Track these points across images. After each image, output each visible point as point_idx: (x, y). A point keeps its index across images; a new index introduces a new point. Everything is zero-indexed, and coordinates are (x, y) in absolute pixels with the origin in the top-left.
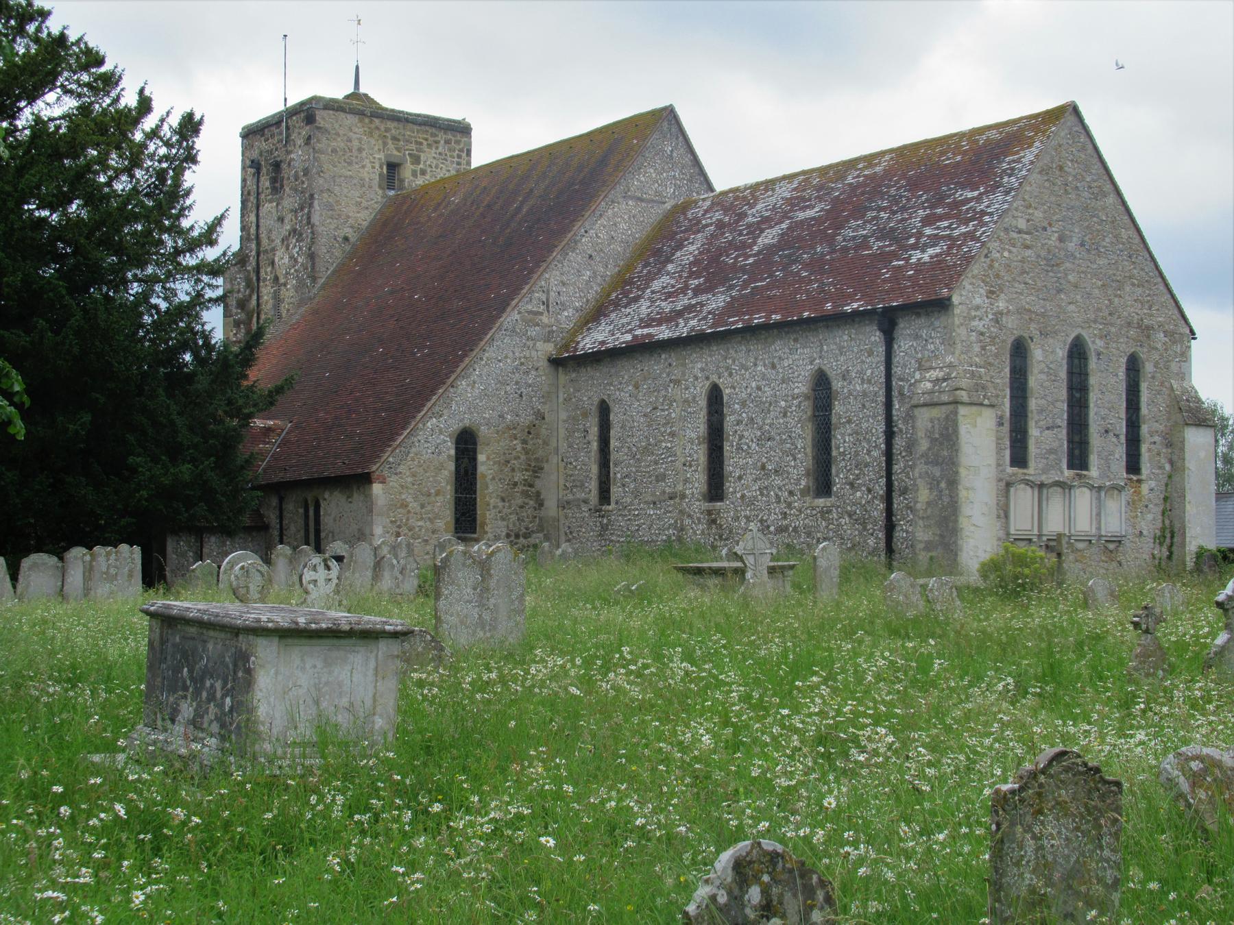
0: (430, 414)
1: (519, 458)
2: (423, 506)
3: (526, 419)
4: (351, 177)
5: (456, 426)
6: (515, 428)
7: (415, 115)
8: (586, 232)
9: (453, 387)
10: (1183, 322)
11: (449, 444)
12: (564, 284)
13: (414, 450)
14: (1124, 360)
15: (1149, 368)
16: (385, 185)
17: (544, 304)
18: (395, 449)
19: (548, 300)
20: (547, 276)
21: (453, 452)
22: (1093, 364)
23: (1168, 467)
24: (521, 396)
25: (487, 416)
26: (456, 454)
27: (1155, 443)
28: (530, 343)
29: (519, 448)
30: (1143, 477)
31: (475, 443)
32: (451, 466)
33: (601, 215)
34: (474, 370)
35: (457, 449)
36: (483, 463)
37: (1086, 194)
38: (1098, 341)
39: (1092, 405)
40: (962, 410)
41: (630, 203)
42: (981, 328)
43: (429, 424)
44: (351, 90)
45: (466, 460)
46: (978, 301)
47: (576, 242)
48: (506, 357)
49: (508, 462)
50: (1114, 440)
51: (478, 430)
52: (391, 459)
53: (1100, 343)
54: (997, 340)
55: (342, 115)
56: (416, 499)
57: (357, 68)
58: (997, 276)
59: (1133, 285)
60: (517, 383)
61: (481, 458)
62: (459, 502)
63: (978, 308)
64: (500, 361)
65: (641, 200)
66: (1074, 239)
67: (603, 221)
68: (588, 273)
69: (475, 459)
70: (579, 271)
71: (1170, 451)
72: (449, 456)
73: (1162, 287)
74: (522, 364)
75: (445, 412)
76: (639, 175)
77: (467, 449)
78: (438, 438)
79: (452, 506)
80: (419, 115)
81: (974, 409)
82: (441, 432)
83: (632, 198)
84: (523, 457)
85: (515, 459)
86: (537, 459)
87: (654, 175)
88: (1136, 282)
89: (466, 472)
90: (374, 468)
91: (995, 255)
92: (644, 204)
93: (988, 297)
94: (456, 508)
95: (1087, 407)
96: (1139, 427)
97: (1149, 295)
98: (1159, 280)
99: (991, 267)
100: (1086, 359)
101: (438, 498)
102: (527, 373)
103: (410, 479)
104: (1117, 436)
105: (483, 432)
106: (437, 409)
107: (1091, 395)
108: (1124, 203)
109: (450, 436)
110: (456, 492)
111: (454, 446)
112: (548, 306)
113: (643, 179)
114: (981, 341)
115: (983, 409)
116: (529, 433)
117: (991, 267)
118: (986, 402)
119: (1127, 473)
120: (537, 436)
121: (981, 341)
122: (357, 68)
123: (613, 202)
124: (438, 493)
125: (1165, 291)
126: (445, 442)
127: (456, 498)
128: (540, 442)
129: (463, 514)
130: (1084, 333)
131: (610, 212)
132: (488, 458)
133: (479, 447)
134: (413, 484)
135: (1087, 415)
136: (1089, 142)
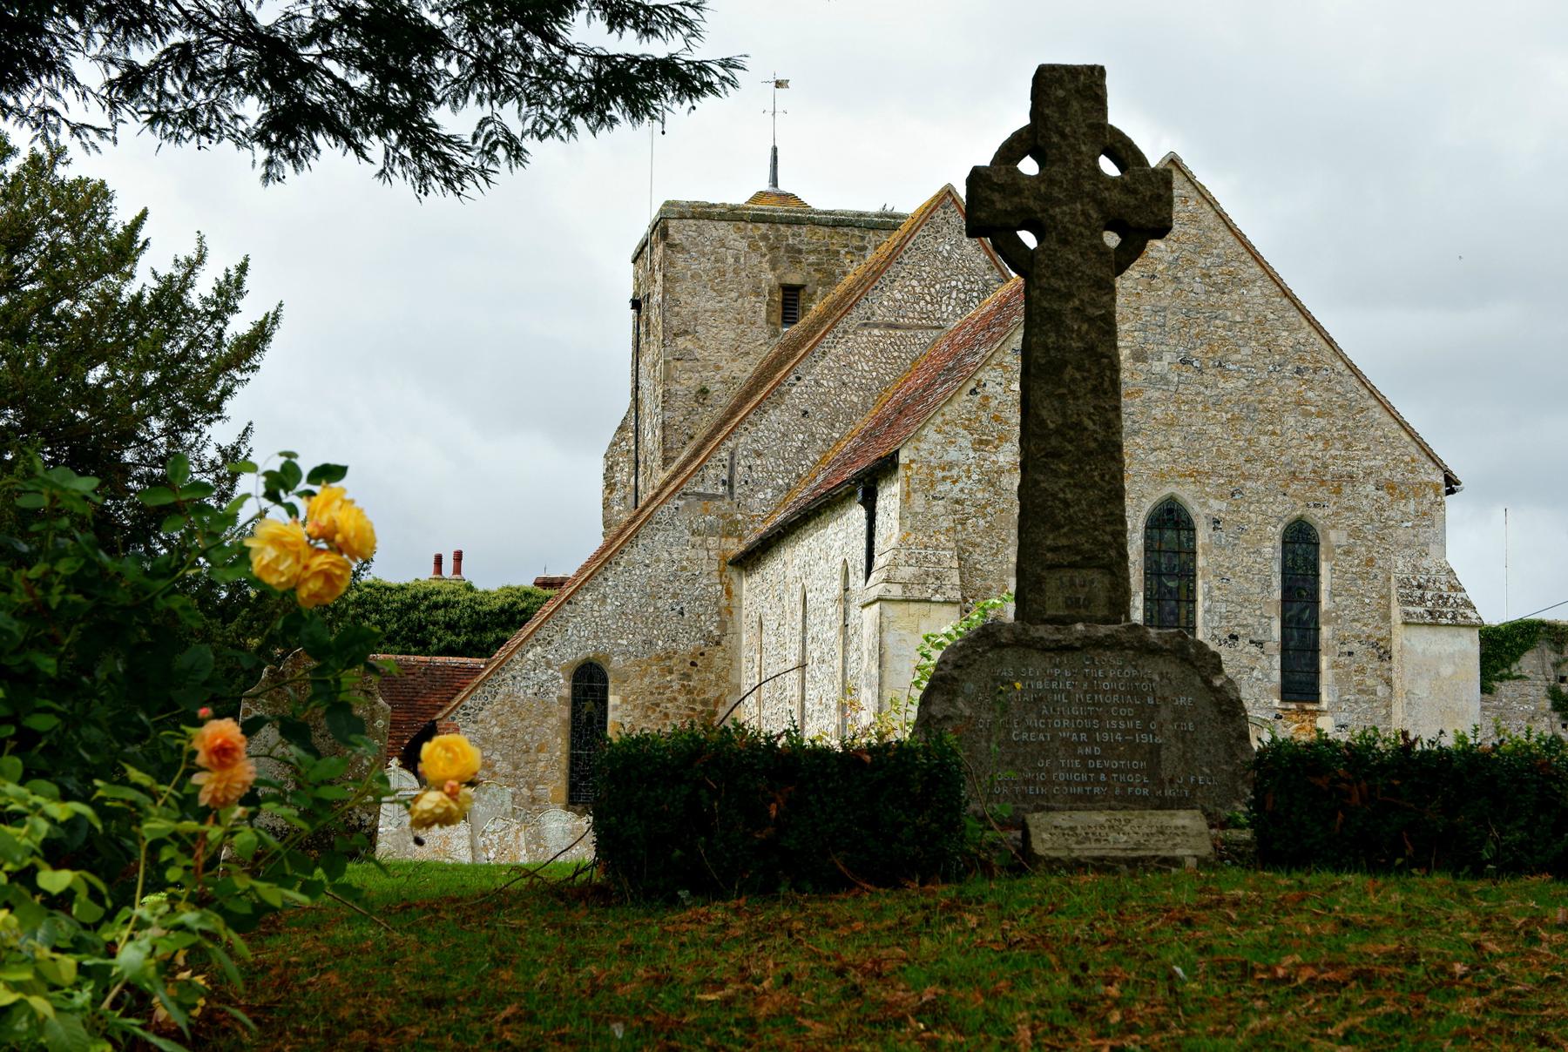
0: (532, 640)
1: (675, 699)
2: (516, 767)
3: (687, 645)
4: (722, 310)
5: (573, 654)
6: (670, 658)
7: (825, 213)
8: (798, 379)
9: (570, 603)
10: (1431, 464)
11: (562, 681)
12: (759, 455)
13: (504, 689)
14: (1275, 532)
15: (1333, 538)
16: (776, 318)
17: (724, 483)
18: (475, 688)
19: (731, 477)
20: (730, 444)
21: (567, 692)
22: (1203, 535)
23: (1381, 690)
24: (682, 614)
25: (625, 642)
26: (574, 694)
27: (1350, 654)
28: (698, 540)
29: (676, 686)
30: (1324, 705)
31: (606, 680)
32: (566, 714)
33: (824, 353)
34: (606, 579)
35: (574, 688)
36: (616, 708)
37: (1197, 287)
38: (1212, 502)
39: (1200, 598)
40: (892, 610)
41: (876, 332)
42: (956, 493)
43: (530, 655)
44: (765, 186)
45: (589, 705)
46: (953, 454)
47: (781, 395)
48: (658, 560)
49: (658, 705)
50: (1254, 649)
51: (608, 659)
52: (468, 703)
53: (1217, 506)
54: (989, 509)
55: (710, 224)
56: (504, 756)
57: (775, 150)
58: (997, 419)
59: (1307, 414)
60: (675, 595)
61: (613, 700)
62: (574, 761)
63: (951, 465)
64: (647, 566)
65: (897, 327)
66: (1167, 357)
67: (828, 361)
68: (801, 436)
69: (605, 702)
70: (784, 435)
71: (1386, 665)
72: (560, 698)
73: (1378, 413)
74: (684, 568)
75: (557, 637)
76: (891, 290)
77: (591, 689)
78: (543, 673)
79: (564, 764)
80: (861, 215)
81: (914, 607)
82: (549, 665)
83: (877, 326)
84: (682, 699)
85: (669, 700)
86: (705, 703)
87: (918, 290)
88: (1313, 410)
89: (590, 718)
90: (440, 715)
91: (990, 388)
92: (899, 333)
93: (975, 450)
94: (572, 770)
95: (1194, 601)
96: (1317, 629)
97: (1344, 427)
98: (1373, 402)
99: (984, 406)
100: (1194, 530)
101: (541, 756)
102: (693, 579)
103: (497, 730)
104: (1260, 644)
105: (617, 662)
106: (543, 634)
107: (1200, 582)
108: (1286, 293)
109: (562, 669)
110: (573, 746)
111: (569, 684)
112: (731, 487)
113: (899, 296)
114: (955, 512)
115: (933, 606)
116: (693, 664)
117: (984, 406)
118: (938, 597)
119: (1283, 699)
120: (708, 668)
121: (955, 512)
122: (775, 150)
123: (845, 332)
124: (539, 750)
125: (1387, 418)
126: (556, 678)
127: (572, 755)
128: (713, 677)
129: (584, 778)
130: (1186, 493)
131: (840, 350)
132: (624, 700)
133: (611, 686)
134: (503, 737)
135: (1194, 612)
136: (1206, 206)
